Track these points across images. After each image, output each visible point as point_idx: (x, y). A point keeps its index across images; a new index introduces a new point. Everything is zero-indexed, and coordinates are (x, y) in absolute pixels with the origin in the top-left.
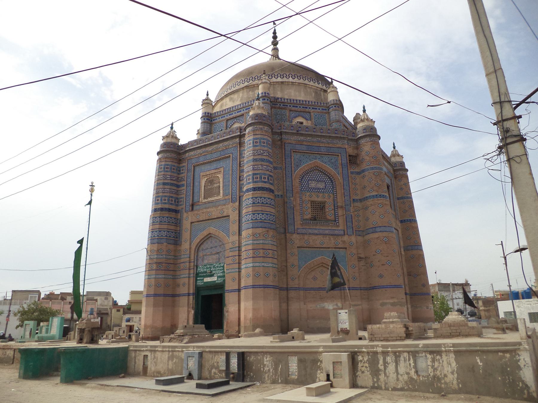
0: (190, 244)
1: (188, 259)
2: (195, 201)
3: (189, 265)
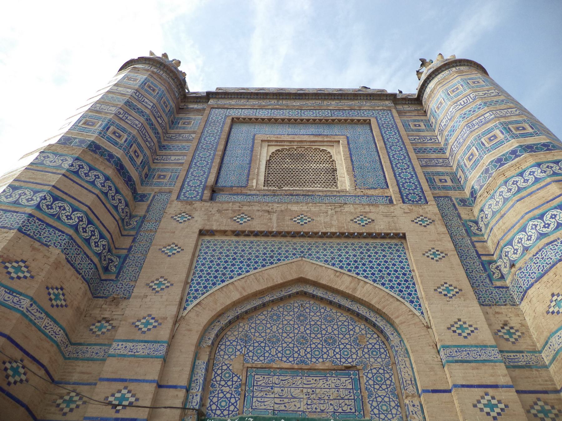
0: (182, 305)
1: (152, 370)
2: (221, 183)
3: (155, 399)
